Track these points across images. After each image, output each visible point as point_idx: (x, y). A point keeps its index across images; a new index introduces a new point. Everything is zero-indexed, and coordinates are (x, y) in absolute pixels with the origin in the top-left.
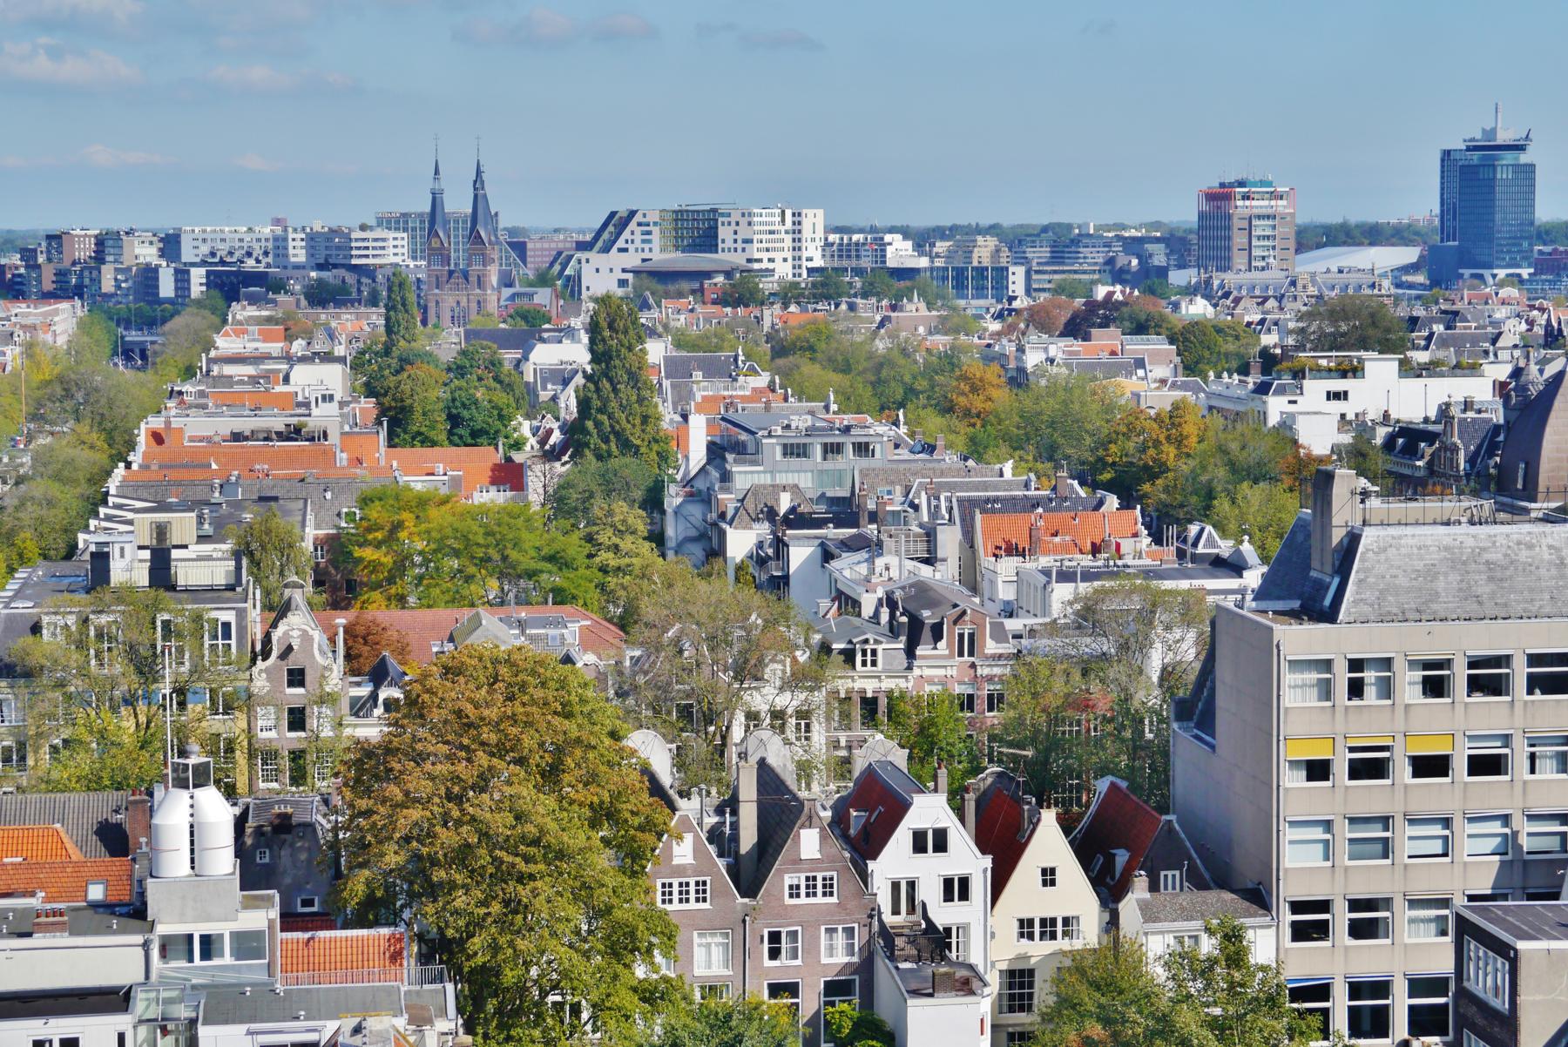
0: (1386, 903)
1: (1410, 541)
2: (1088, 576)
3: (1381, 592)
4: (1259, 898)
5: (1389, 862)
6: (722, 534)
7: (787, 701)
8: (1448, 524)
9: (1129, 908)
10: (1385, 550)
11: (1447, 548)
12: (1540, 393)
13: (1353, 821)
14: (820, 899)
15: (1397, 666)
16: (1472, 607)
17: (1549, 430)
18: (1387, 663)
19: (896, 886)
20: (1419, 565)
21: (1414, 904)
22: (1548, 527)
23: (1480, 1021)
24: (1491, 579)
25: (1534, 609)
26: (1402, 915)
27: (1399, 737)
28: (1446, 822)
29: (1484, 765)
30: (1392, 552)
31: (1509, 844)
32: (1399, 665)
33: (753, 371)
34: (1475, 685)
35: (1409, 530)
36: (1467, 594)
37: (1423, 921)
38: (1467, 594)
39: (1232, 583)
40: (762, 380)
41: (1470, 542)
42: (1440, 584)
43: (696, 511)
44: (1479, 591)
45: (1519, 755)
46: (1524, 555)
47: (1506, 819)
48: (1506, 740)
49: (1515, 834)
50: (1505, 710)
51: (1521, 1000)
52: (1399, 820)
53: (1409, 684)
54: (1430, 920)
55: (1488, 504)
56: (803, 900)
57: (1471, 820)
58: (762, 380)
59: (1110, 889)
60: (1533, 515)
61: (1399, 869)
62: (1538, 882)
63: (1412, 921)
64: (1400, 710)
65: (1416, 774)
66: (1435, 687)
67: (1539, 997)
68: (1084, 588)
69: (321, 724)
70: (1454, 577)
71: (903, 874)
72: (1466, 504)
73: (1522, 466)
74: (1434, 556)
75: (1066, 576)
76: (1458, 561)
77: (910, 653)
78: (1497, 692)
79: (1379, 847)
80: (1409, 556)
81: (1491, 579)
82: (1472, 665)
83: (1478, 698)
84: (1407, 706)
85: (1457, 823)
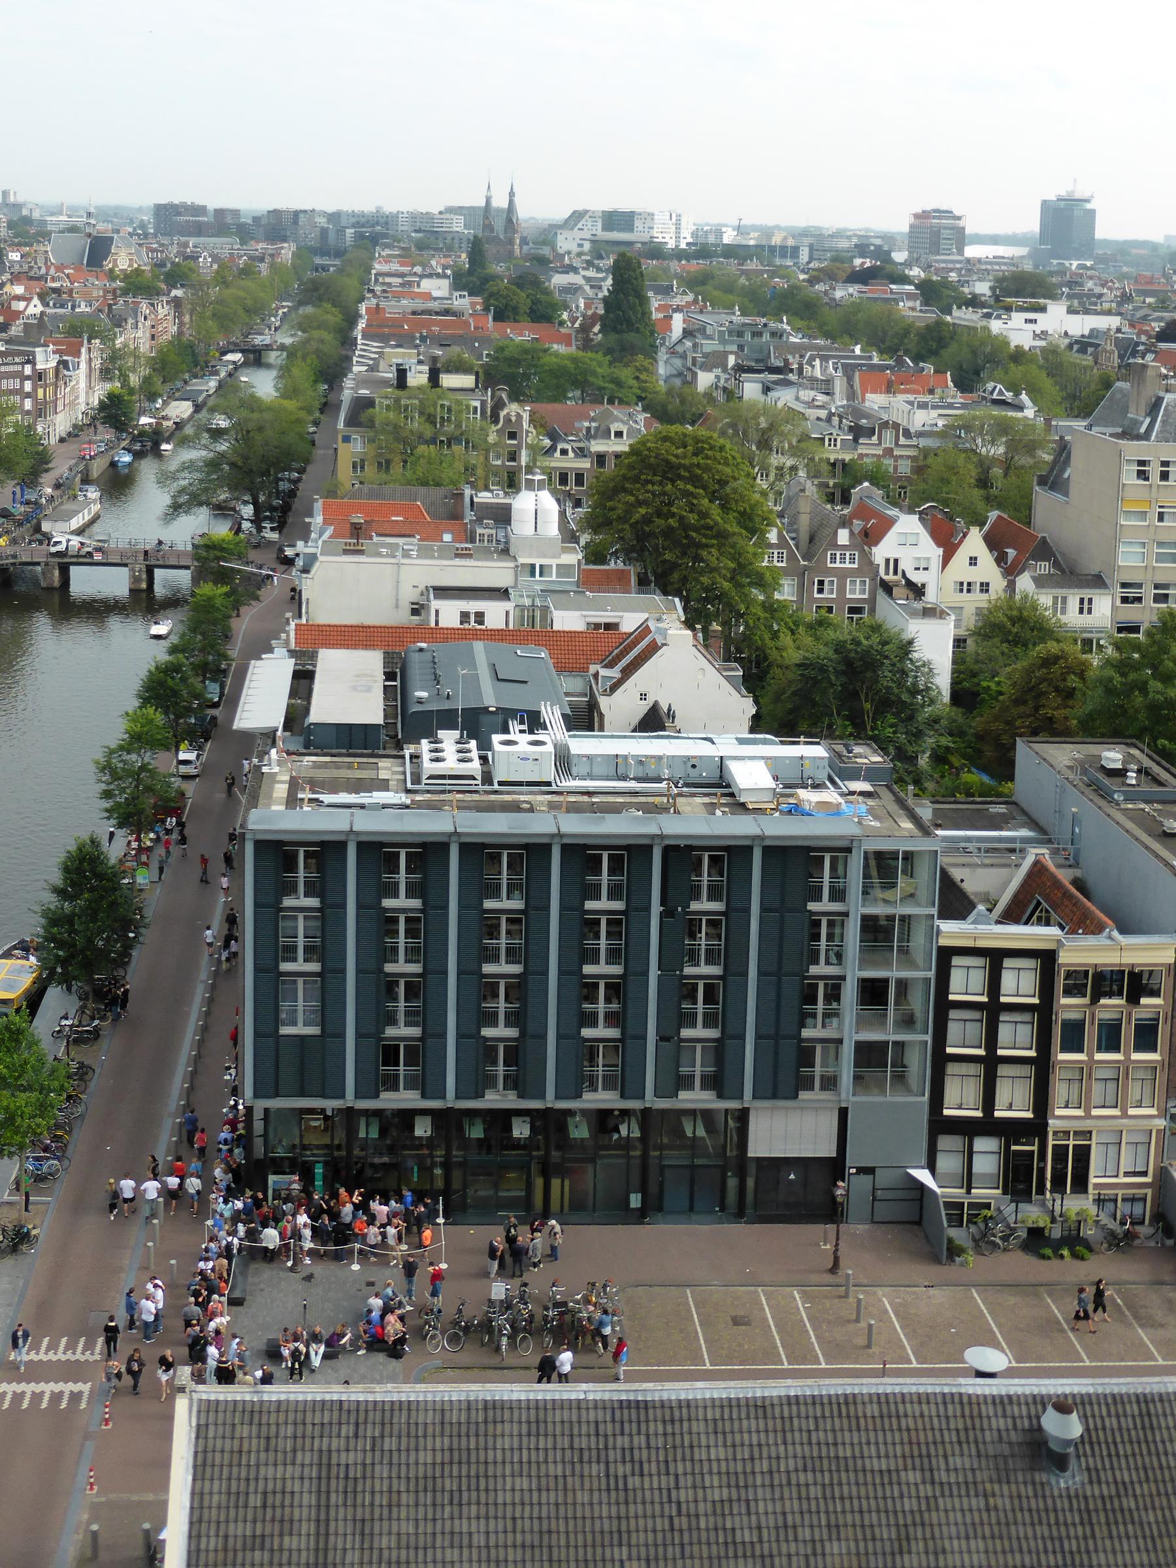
2: (934, 407)
4: (1098, 582)
6: (695, 375)
7: (789, 463)
9: (1025, 582)
14: (847, 565)
19: (887, 561)
33: (684, 293)
39: (1019, 415)
40: (690, 297)
43: (678, 362)
56: (838, 565)
58: (690, 297)
59: (1010, 571)
68: (934, 413)
69: (524, 458)
71: (892, 556)
75: (923, 406)
77: (856, 440)
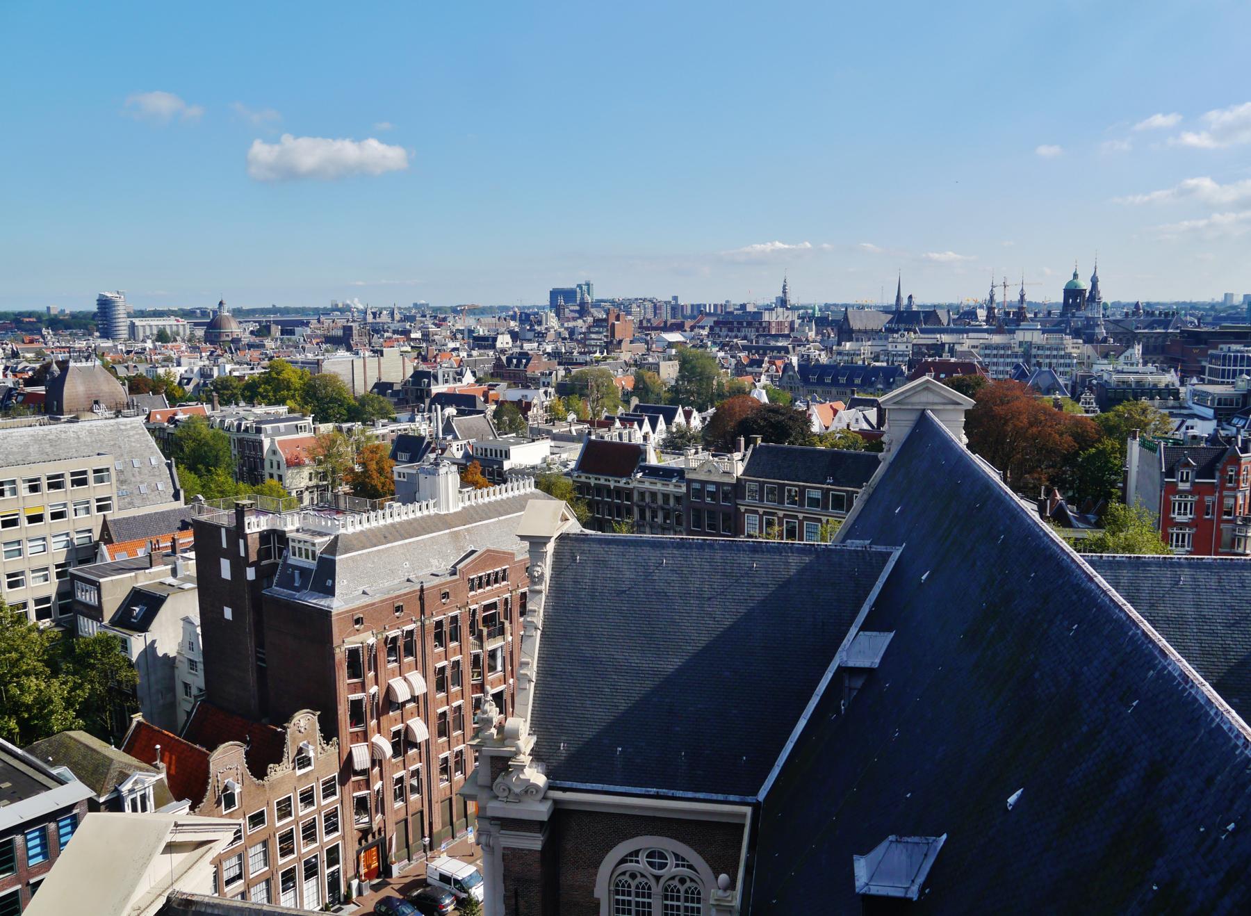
0: (22, 573)
1: (17, 434)
3: (7, 454)
5: (21, 557)
8: (31, 426)
10: (6, 438)
11: (32, 436)
12: (59, 375)
13: (5, 544)
15: (17, 482)
16: (45, 457)
17: (65, 388)
18: (13, 482)
20: (21, 443)
21: (33, 571)
22: (72, 425)
23: (85, 611)
24: (51, 446)
25: (70, 455)
26: (29, 576)
27: (22, 510)
28: (44, 539)
29: (55, 516)
30: (9, 439)
31: (69, 543)
32: (19, 482)
34: (51, 486)
35: (16, 430)
36: (42, 452)
37: (38, 577)
38: (42, 452)
41: (42, 432)
42: (31, 450)
44: (47, 450)
45: (71, 508)
46: (63, 436)
47: (67, 534)
48: (65, 505)
49: (72, 539)
50: (63, 494)
51: (104, 599)
52: (24, 540)
53: (23, 489)
54: (40, 576)
55: (46, 417)
57: (54, 537)
60: (66, 420)
61: (26, 560)
62: (82, 556)
63: (33, 578)
64: (21, 500)
65: (29, 523)
66: (34, 489)
67: (110, 598)
70: (36, 446)
72: (37, 418)
73: (55, 403)
74: (27, 439)
76: (36, 440)
78: (59, 487)
79: (17, 552)
80: (17, 440)
81: (51, 446)
82: (48, 479)
83: (52, 491)
84: (24, 497)
85: (48, 539)
